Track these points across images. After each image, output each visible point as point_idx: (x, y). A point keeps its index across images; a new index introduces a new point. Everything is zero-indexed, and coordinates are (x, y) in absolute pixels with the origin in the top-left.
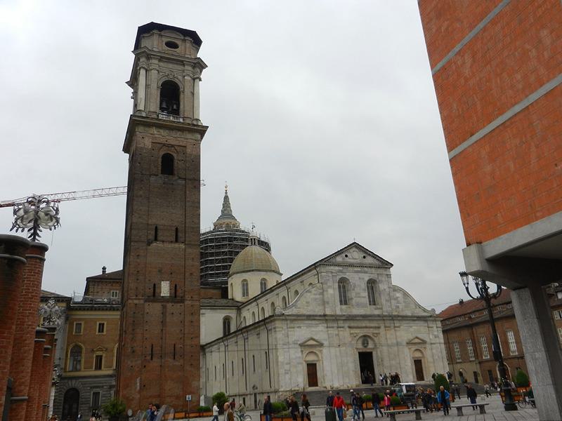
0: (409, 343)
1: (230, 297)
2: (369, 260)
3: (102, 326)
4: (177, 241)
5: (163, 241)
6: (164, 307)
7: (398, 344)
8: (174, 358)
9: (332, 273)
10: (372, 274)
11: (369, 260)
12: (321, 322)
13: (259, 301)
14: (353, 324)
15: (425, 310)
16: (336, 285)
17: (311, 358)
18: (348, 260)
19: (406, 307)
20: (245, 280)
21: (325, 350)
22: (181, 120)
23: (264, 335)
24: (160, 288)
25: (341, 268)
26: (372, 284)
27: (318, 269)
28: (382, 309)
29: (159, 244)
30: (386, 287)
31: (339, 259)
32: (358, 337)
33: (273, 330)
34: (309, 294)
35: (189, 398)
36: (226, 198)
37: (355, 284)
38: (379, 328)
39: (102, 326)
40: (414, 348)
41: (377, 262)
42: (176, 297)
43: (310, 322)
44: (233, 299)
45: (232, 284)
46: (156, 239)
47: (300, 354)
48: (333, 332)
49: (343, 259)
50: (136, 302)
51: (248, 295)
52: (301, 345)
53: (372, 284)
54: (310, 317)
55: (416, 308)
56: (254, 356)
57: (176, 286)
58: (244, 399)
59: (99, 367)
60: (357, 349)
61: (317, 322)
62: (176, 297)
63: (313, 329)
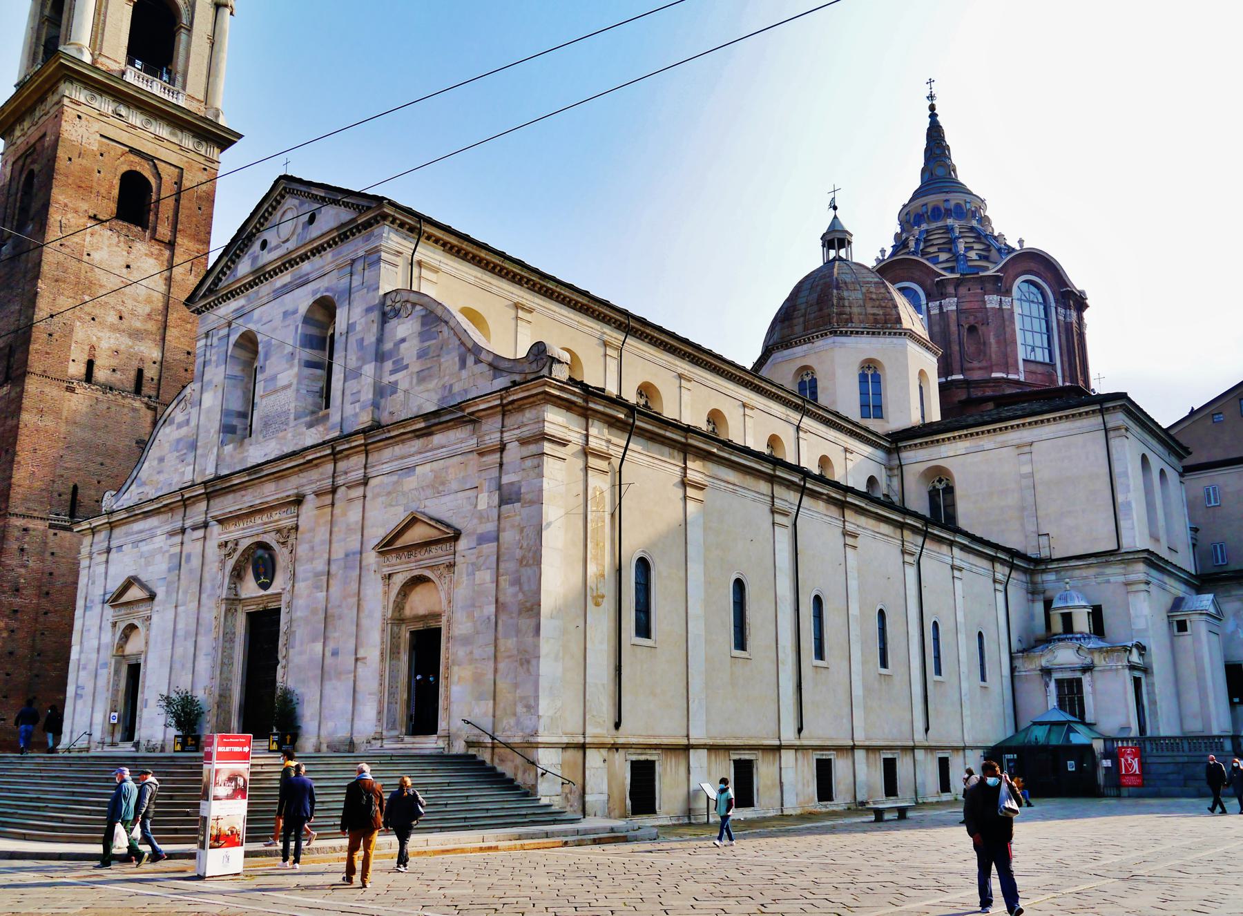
0: (388, 546)
2: (330, 217)
10: (324, 276)
12: (162, 517)
18: (266, 257)
19: (422, 377)
31: (244, 268)
32: (236, 556)
37: (268, 344)
38: (299, 501)
40: (404, 569)
61: (153, 522)
63: (144, 547)
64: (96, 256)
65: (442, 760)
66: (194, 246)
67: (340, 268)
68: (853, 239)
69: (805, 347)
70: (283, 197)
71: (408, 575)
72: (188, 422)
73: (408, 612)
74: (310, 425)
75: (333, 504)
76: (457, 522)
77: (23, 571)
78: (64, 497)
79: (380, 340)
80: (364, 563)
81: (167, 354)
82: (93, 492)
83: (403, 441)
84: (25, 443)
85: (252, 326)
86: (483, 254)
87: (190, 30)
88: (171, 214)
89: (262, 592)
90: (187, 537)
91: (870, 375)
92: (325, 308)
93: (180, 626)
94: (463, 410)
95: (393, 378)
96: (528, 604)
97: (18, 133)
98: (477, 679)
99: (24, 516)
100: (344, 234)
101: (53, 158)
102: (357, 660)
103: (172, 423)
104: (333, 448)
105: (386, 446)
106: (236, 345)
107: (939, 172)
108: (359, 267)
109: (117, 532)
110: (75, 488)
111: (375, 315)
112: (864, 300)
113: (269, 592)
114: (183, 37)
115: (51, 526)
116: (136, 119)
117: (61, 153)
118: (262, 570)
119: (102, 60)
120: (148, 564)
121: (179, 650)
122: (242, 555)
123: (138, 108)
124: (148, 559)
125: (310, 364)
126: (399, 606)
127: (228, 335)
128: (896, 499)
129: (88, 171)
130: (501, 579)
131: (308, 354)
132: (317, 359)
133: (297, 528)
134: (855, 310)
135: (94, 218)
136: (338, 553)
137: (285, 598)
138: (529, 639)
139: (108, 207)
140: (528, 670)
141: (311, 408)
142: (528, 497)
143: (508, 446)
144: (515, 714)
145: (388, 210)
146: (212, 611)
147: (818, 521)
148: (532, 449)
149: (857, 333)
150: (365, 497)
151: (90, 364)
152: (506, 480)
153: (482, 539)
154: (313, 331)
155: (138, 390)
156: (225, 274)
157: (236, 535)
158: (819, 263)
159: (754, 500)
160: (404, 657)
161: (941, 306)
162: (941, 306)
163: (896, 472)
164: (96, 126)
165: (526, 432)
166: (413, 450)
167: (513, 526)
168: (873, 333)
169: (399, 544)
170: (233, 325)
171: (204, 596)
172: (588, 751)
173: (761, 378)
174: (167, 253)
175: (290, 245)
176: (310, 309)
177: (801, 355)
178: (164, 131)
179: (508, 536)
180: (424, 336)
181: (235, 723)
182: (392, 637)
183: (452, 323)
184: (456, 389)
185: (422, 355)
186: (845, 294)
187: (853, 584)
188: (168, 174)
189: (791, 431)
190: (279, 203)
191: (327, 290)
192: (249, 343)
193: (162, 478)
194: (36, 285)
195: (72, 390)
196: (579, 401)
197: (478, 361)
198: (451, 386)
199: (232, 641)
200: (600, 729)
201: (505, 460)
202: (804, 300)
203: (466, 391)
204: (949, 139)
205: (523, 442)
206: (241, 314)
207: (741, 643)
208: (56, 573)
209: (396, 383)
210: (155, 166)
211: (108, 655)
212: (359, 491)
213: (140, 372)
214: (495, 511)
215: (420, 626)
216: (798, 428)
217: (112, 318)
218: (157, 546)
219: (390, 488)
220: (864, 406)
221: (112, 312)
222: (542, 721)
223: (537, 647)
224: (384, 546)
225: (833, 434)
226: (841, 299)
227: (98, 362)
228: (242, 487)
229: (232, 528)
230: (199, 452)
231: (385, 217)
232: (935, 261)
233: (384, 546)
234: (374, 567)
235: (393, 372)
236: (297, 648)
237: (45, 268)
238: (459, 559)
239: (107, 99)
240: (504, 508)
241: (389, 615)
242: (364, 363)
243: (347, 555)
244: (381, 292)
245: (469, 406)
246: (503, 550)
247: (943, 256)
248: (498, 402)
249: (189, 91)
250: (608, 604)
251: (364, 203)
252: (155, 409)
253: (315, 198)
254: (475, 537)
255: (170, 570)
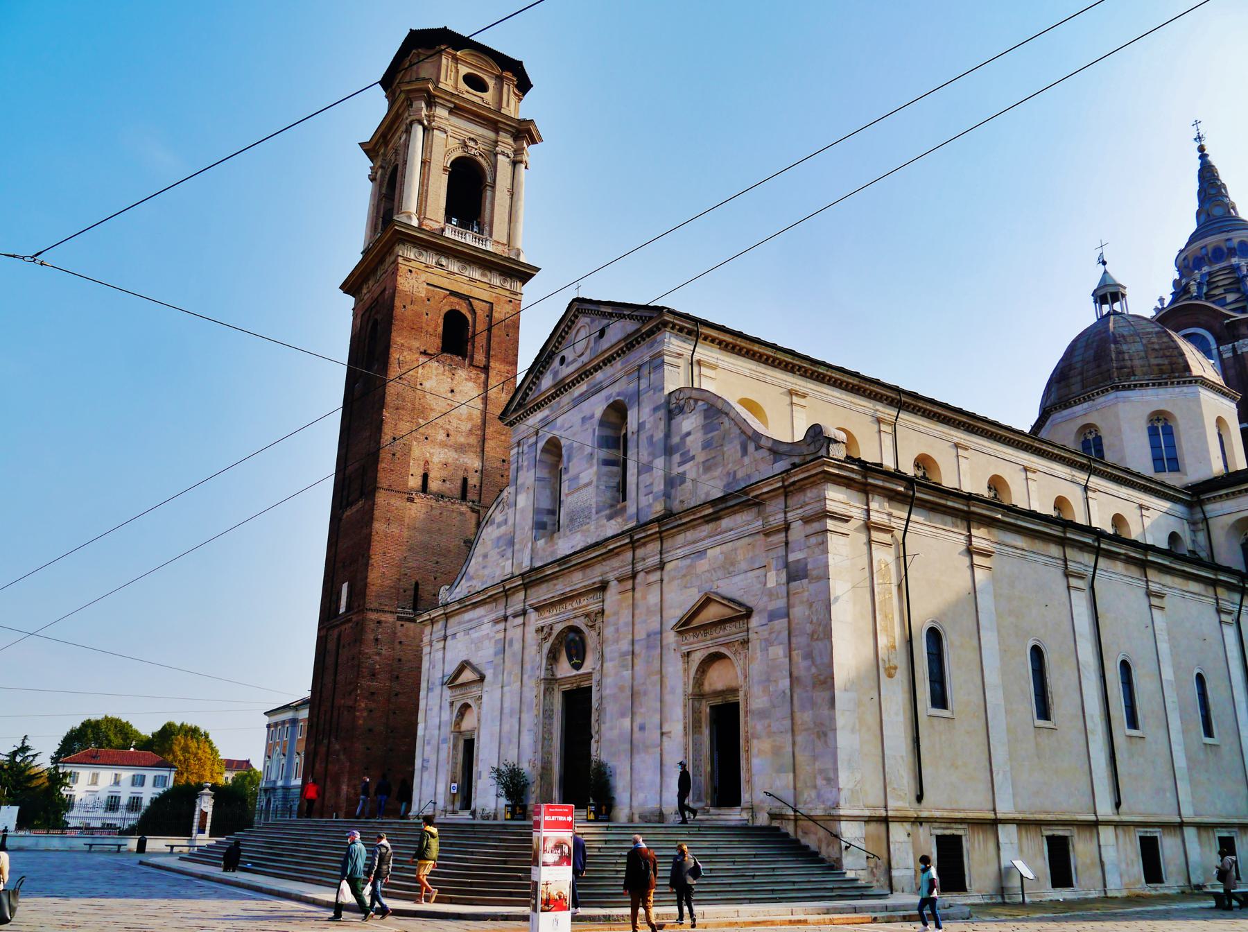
0: (685, 626)
10: (615, 382)
14: (542, 593)
18: (566, 371)
19: (708, 467)
30: (646, 410)
31: (547, 382)
38: (603, 587)
40: (701, 647)
49: (556, 374)
55: (745, 451)
63: (475, 635)
64: (428, 385)
65: (747, 832)
66: (504, 368)
67: (628, 374)
68: (1127, 292)
69: (1085, 405)
70: (576, 317)
71: (706, 652)
72: (506, 521)
73: (707, 688)
74: (610, 518)
75: (634, 589)
76: (749, 601)
77: (378, 658)
78: (408, 593)
79: (668, 436)
80: (665, 642)
81: (486, 464)
82: (430, 588)
83: (694, 527)
84: (377, 547)
85: (556, 433)
86: (756, 348)
87: (493, 187)
88: (484, 342)
89: (575, 672)
90: (509, 623)
91: (1161, 429)
92: (618, 411)
93: (506, 705)
94: (748, 494)
95: (681, 470)
96: (822, 678)
97: (365, 291)
98: (776, 751)
99: (377, 611)
100: (630, 343)
101: (392, 307)
102: (662, 734)
103: (493, 523)
104: (632, 537)
105: (679, 533)
106: (544, 450)
107: (1217, 212)
108: (645, 371)
109: (452, 621)
110: (417, 584)
111: (661, 413)
112: (1146, 352)
113: (581, 672)
114: (489, 193)
115: (399, 619)
116: (454, 267)
117: (398, 303)
118: (574, 652)
119: (426, 222)
120: (478, 649)
121: (506, 727)
122: (556, 638)
123: (455, 257)
124: (478, 643)
125: (607, 463)
126: (699, 682)
127: (536, 443)
128: (1203, 554)
129: (419, 315)
130: (794, 653)
131: (603, 453)
132: (612, 458)
133: (602, 612)
134: (1137, 362)
135: (424, 353)
136: (641, 634)
137: (595, 677)
138: (826, 712)
139: (435, 343)
140: (826, 742)
141: (609, 502)
142: (814, 573)
143: (793, 526)
144: (815, 787)
145: (668, 318)
146: (533, 690)
147: (1117, 582)
148: (816, 526)
149: (1141, 385)
150: (662, 580)
151: (425, 477)
152: (792, 557)
153: (773, 616)
154: (609, 432)
155: (464, 497)
156: (531, 389)
157: (551, 620)
158: (1092, 319)
159: (1045, 565)
160: (706, 731)
161: (1234, 350)
162: (1234, 350)
163: (1200, 526)
164: (424, 277)
165: (809, 510)
166: (704, 534)
167: (802, 602)
168: (1160, 384)
169: (695, 623)
170: (541, 433)
171: (525, 677)
172: (892, 825)
173: (1041, 441)
174: (483, 376)
175: (585, 359)
176: (605, 413)
177: (1081, 414)
178: (476, 274)
179: (798, 612)
180: (707, 428)
181: (556, 794)
182: (694, 712)
183: (732, 414)
184: (740, 475)
185: (707, 445)
186: (1125, 347)
187: (1164, 647)
188: (480, 308)
189: (1079, 491)
190: (573, 322)
191: (619, 394)
192: (554, 448)
193: (486, 572)
194: (381, 414)
195: (411, 500)
196: (858, 477)
197: (758, 447)
198: (735, 472)
199: (551, 717)
200: (901, 803)
201: (790, 539)
202: (1080, 358)
203: (749, 476)
204: (1224, 177)
205: (807, 520)
206: (546, 423)
207: (1044, 711)
208: (403, 659)
209: (684, 473)
210: (470, 304)
211: (447, 731)
212: (656, 576)
213: (465, 480)
214: (784, 588)
215: (719, 701)
216: (1086, 488)
217: (441, 436)
218: (485, 633)
219: (684, 572)
220: (1157, 460)
221: (441, 431)
222: (842, 793)
223: (833, 719)
224: (682, 626)
225: (1124, 491)
226: (1120, 353)
227: (431, 475)
228: (554, 577)
229: (547, 614)
230: (516, 547)
231: (665, 324)
232: (1223, 303)
233: (682, 626)
234: (673, 646)
235: (680, 464)
236: (608, 725)
237: (388, 399)
238: (752, 636)
239: (431, 253)
240: (793, 584)
241: (690, 690)
242: (655, 457)
243: (649, 636)
244: (666, 392)
245: (753, 490)
246: (793, 625)
247: (1231, 297)
248: (780, 484)
249: (495, 237)
250: (901, 675)
251: (647, 314)
252: (478, 512)
253: (604, 315)
254: (766, 615)
255: (496, 654)
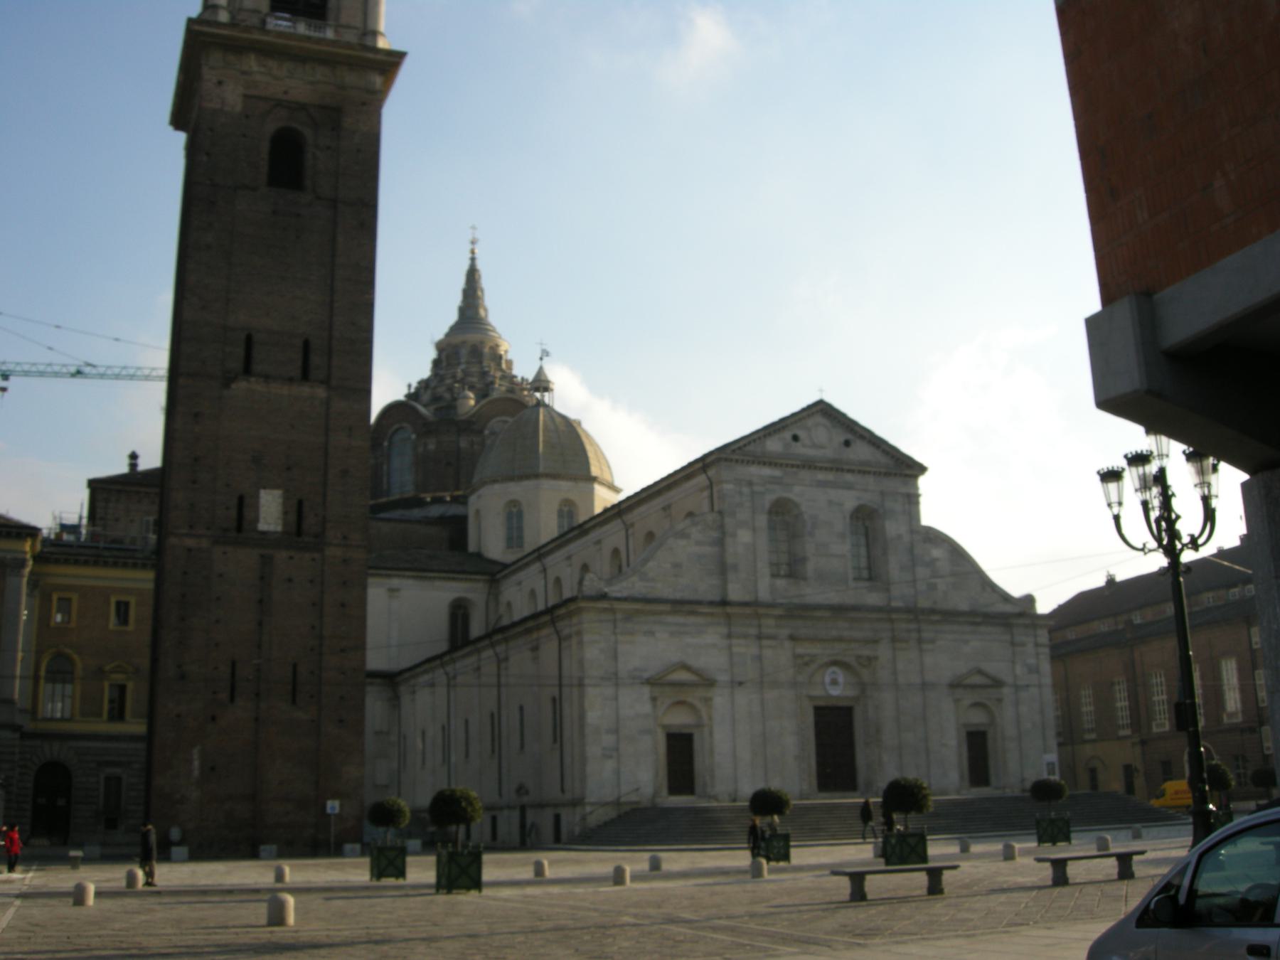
1: (472, 548)
3: (123, 609)
4: (305, 376)
5: (267, 378)
6: (266, 561)
7: (925, 686)
8: (294, 702)
9: (750, 484)
11: (860, 452)
13: (549, 560)
15: (1006, 597)
16: (762, 520)
17: (679, 719)
18: (798, 449)
20: (514, 503)
21: (720, 699)
22: (330, 34)
23: (549, 648)
24: (256, 507)
25: (777, 473)
26: (865, 520)
27: (711, 472)
28: (888, 590)
29: (256, 385)
31: (774, 445)
33: (574, 640)
34: (683, 542)
35: (333, 808)
36: (472, 276)
38: (876, 641)
39: (123, 609)
41: (883, 459)
42: (299, 532)
43: (680, 619)
44: (479, 555)
45: (478, 512)
46: (247, 370)
47: (647, 708)
48: (744, 649)
50: (190, 542)
51: (521, 546)
52: (651, 682)
53: (865, 520)
54: (681, 605)
56: (521, 708)
57: (300, 503)
58: (494, 819)
59: (118, 713)
60: (811, 698)
61: (700, 620)
62: (299, 532)
